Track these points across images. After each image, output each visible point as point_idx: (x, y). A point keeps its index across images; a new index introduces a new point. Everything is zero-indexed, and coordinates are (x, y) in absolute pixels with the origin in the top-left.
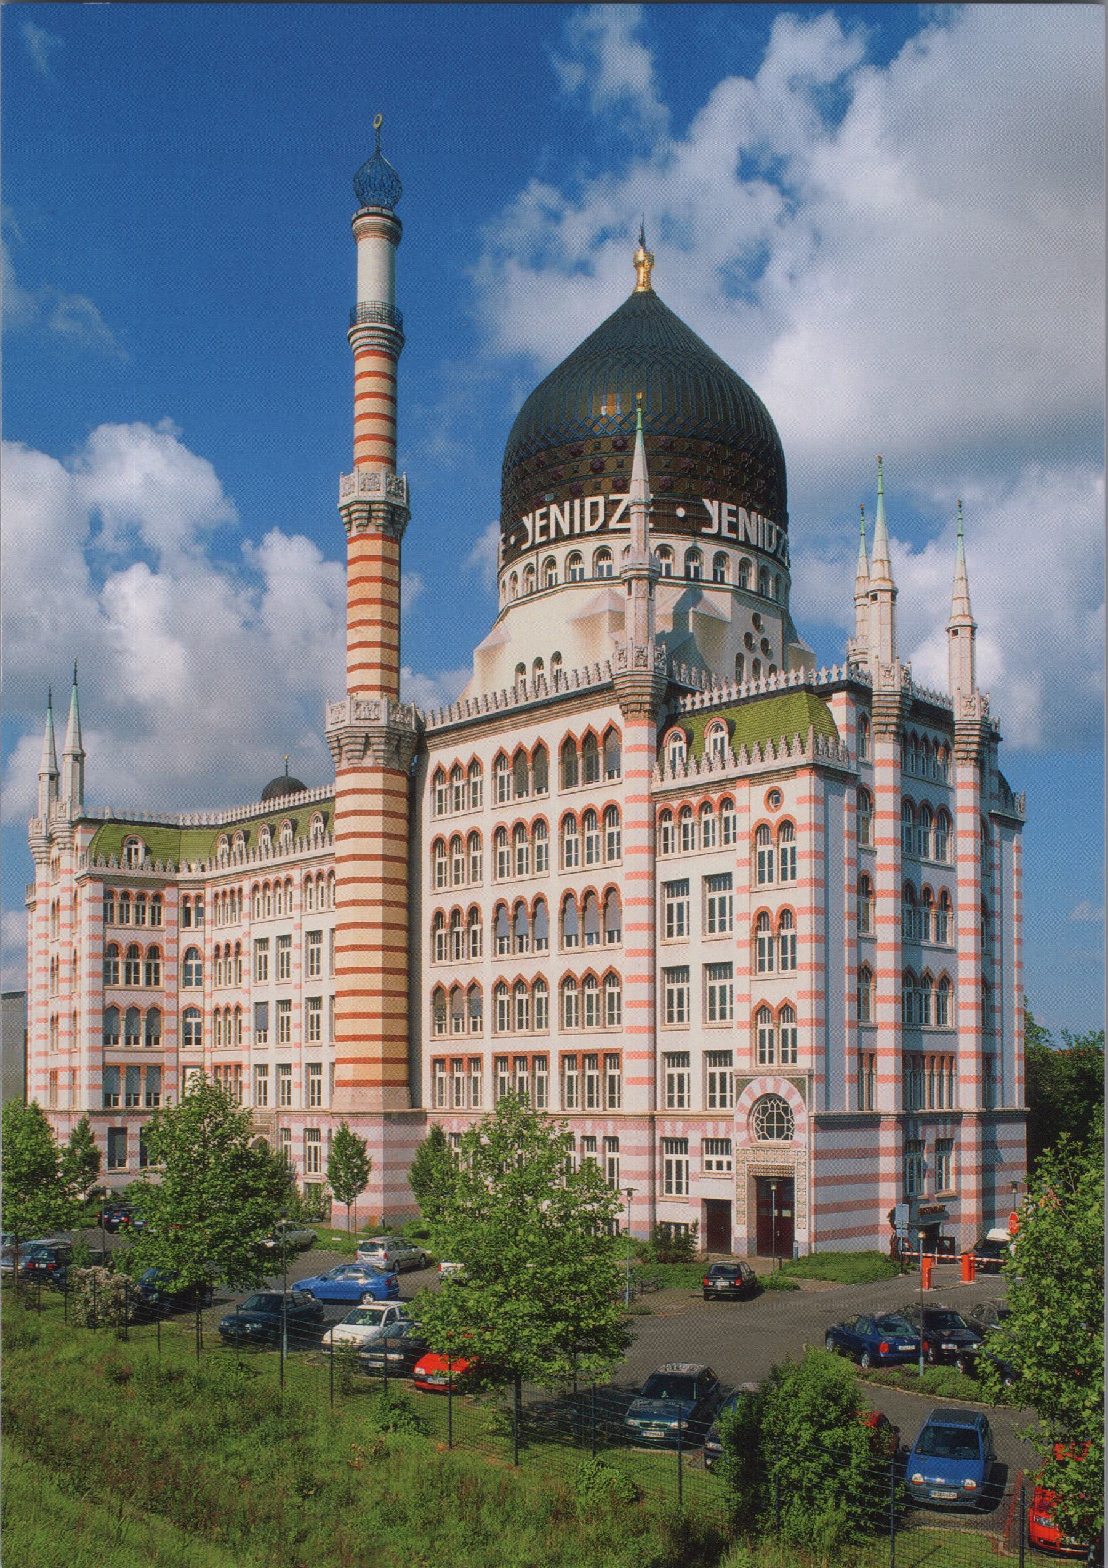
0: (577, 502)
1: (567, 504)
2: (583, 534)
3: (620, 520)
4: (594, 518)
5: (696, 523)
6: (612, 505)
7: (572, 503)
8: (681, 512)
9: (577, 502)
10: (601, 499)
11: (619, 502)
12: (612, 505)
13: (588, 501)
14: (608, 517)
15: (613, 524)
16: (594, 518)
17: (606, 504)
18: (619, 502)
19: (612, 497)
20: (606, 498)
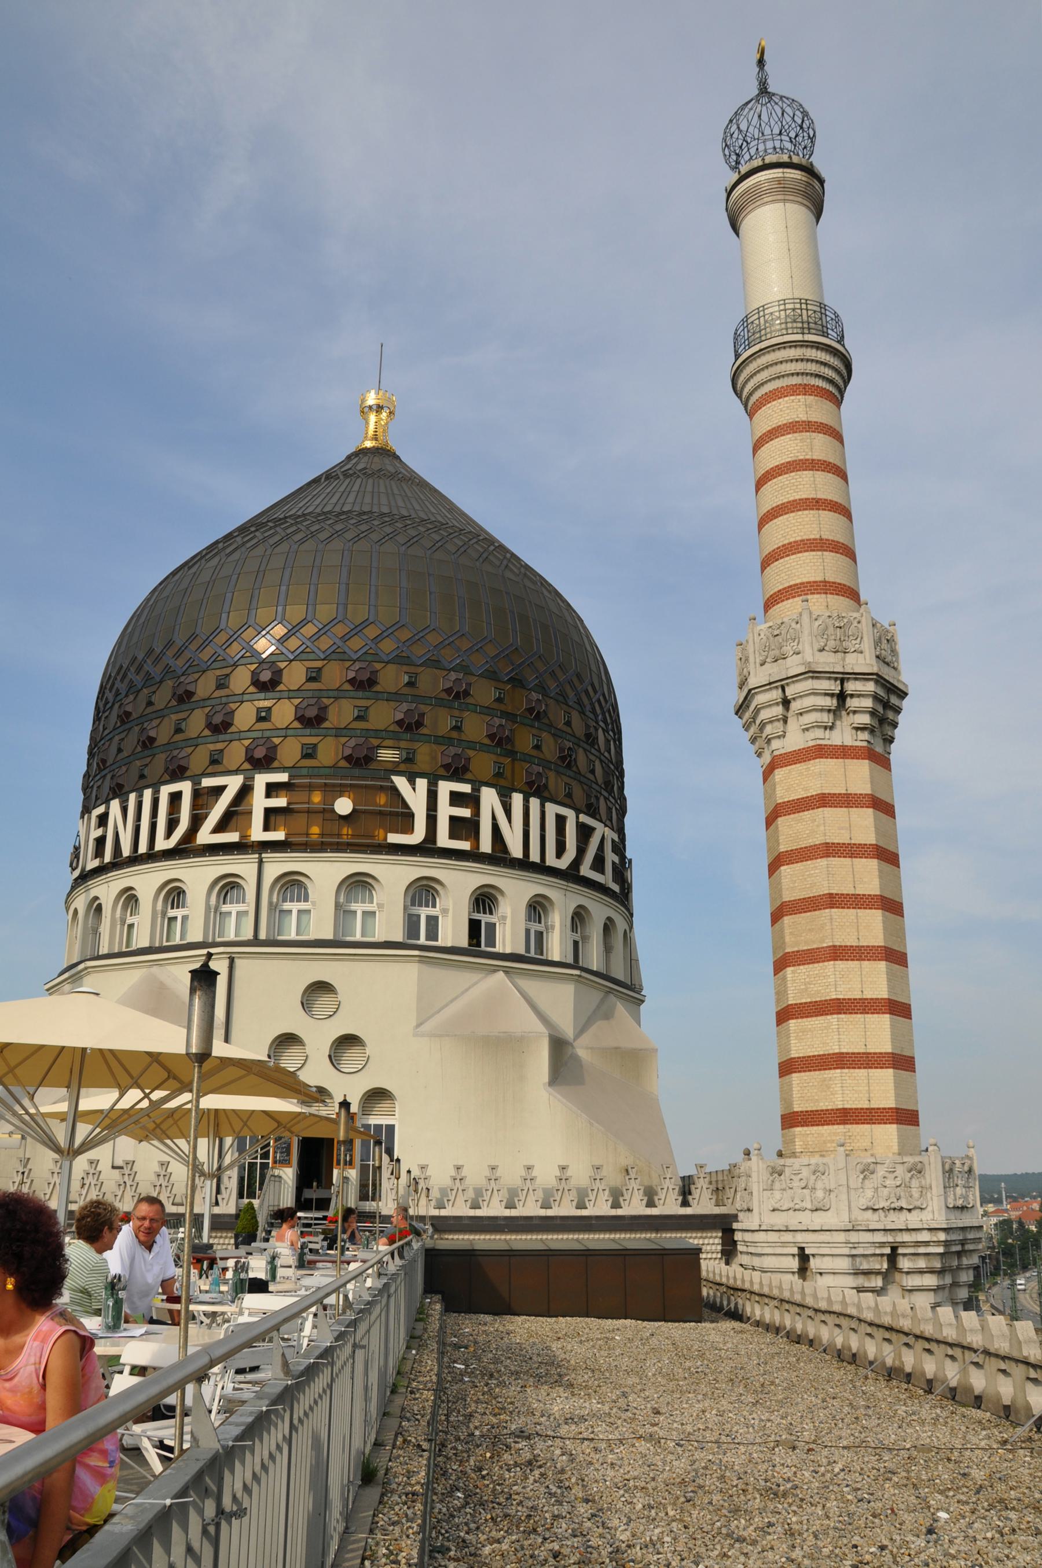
0: (148, 794)
1: (132, 797)
2: (152, 856)
3: (219, 828)
4: (172, 824)
5: (372, 830)
6: (203, 798)
7: (141, 796)
8: (344, 806)
9: (148, 794)
10: (185, 787)
11: (220, 790)
12: (203, 798)
13: (166, 791)
14: (196, 822)
15: (205, 836)
16: (172, 824)
17: (197, 794)
18: (220, 790)
19: (207, 782)
20: (196, 783)
